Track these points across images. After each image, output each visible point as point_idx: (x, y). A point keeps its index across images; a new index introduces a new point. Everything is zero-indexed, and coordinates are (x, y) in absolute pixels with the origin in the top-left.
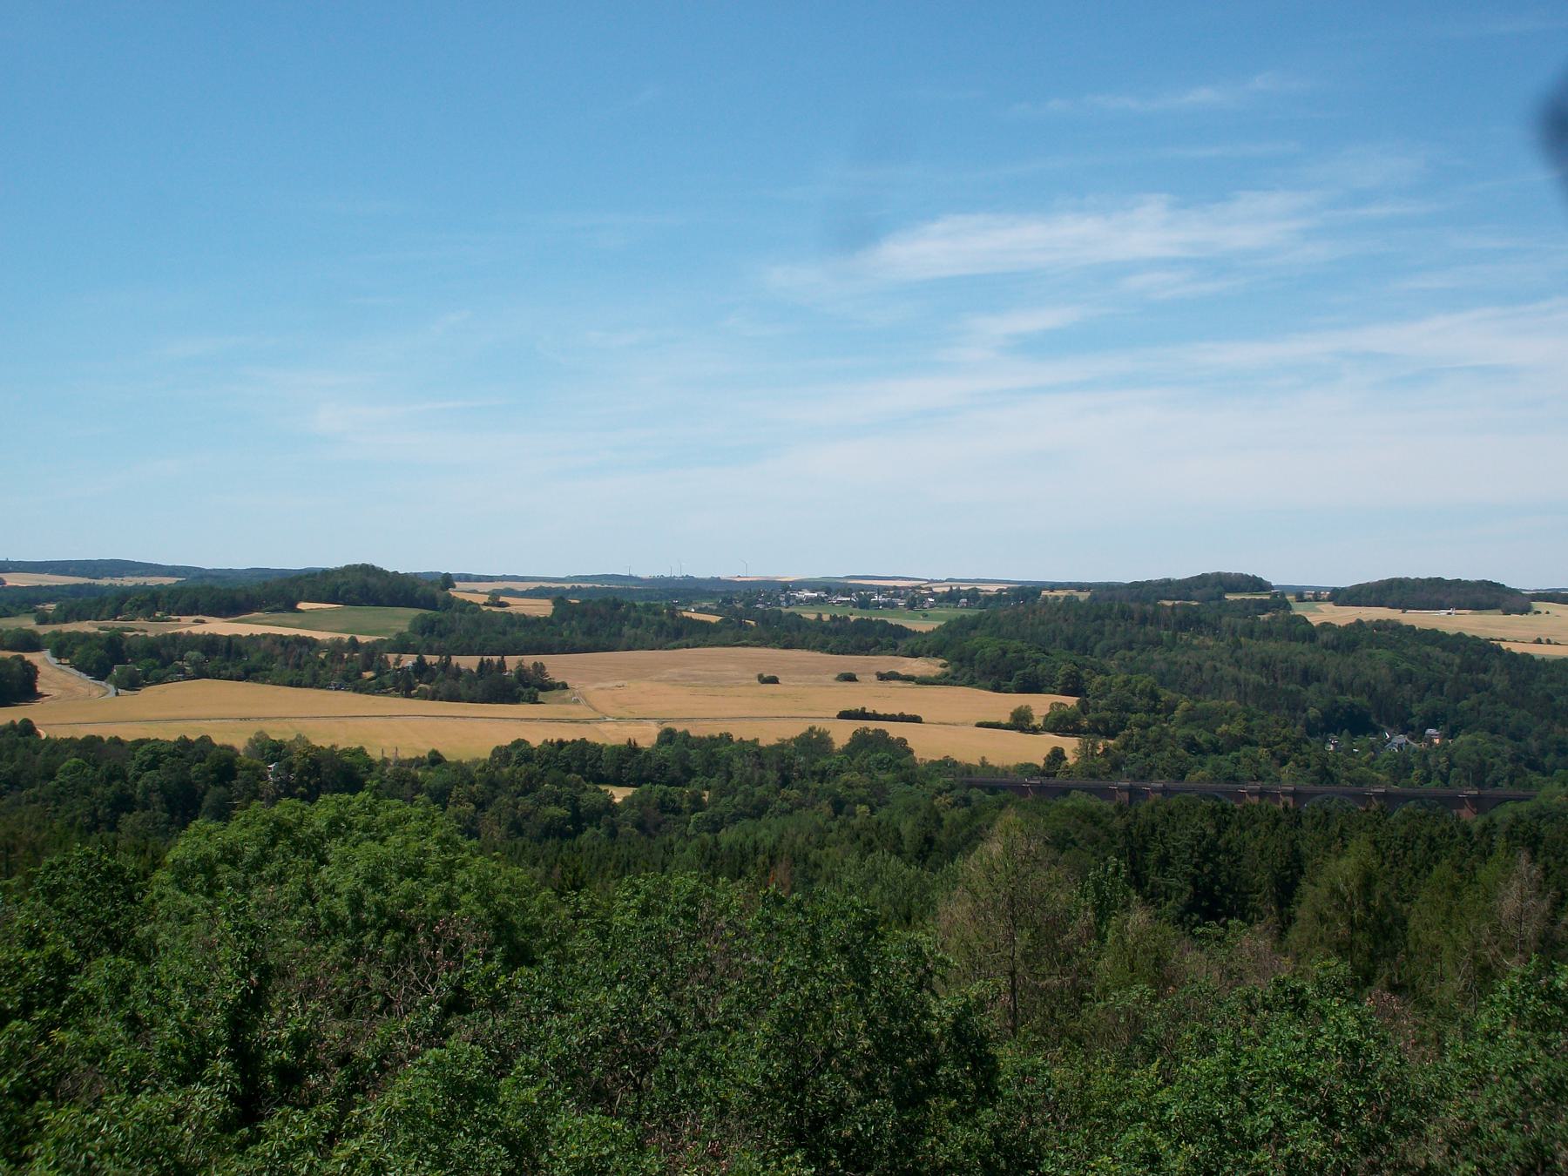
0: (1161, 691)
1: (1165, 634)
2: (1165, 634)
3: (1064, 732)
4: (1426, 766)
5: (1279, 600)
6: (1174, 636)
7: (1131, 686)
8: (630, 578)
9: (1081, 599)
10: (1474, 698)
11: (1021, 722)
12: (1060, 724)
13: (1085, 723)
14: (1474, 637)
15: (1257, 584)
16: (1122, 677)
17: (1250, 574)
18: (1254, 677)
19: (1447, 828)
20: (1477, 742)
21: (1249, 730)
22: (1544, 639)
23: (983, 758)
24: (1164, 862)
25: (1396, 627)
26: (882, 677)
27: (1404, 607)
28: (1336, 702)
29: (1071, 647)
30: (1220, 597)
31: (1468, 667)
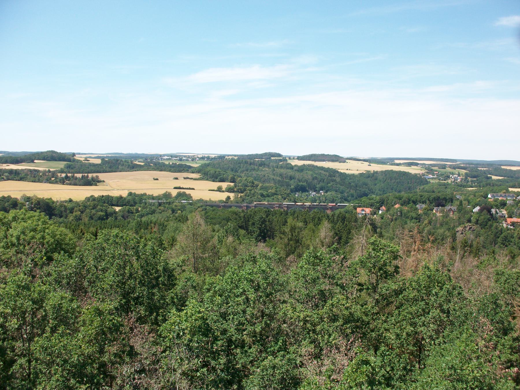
0: (255, 182)
1: (256, 167)
2: (256, 167)
3: (231, 192)
4: (320, 200)
5: (285, 160)
6: (258, 168)
7: (247, 180)
8: (121, 153)
10: (332, 183)
11: (220, 190)
12: (230, 190)
13: (236, 190)
14: (332, 169)
15: (279, 155)
16: (245, 178)
18: (278, 178)
19: (323, 215)
21: (276, 191)
24: (253, 224)
25: (313, 166)
26: (185, 178)
27: (315, 161)
29: (232, 171)
30: (270, 158)
31: (330, 176)
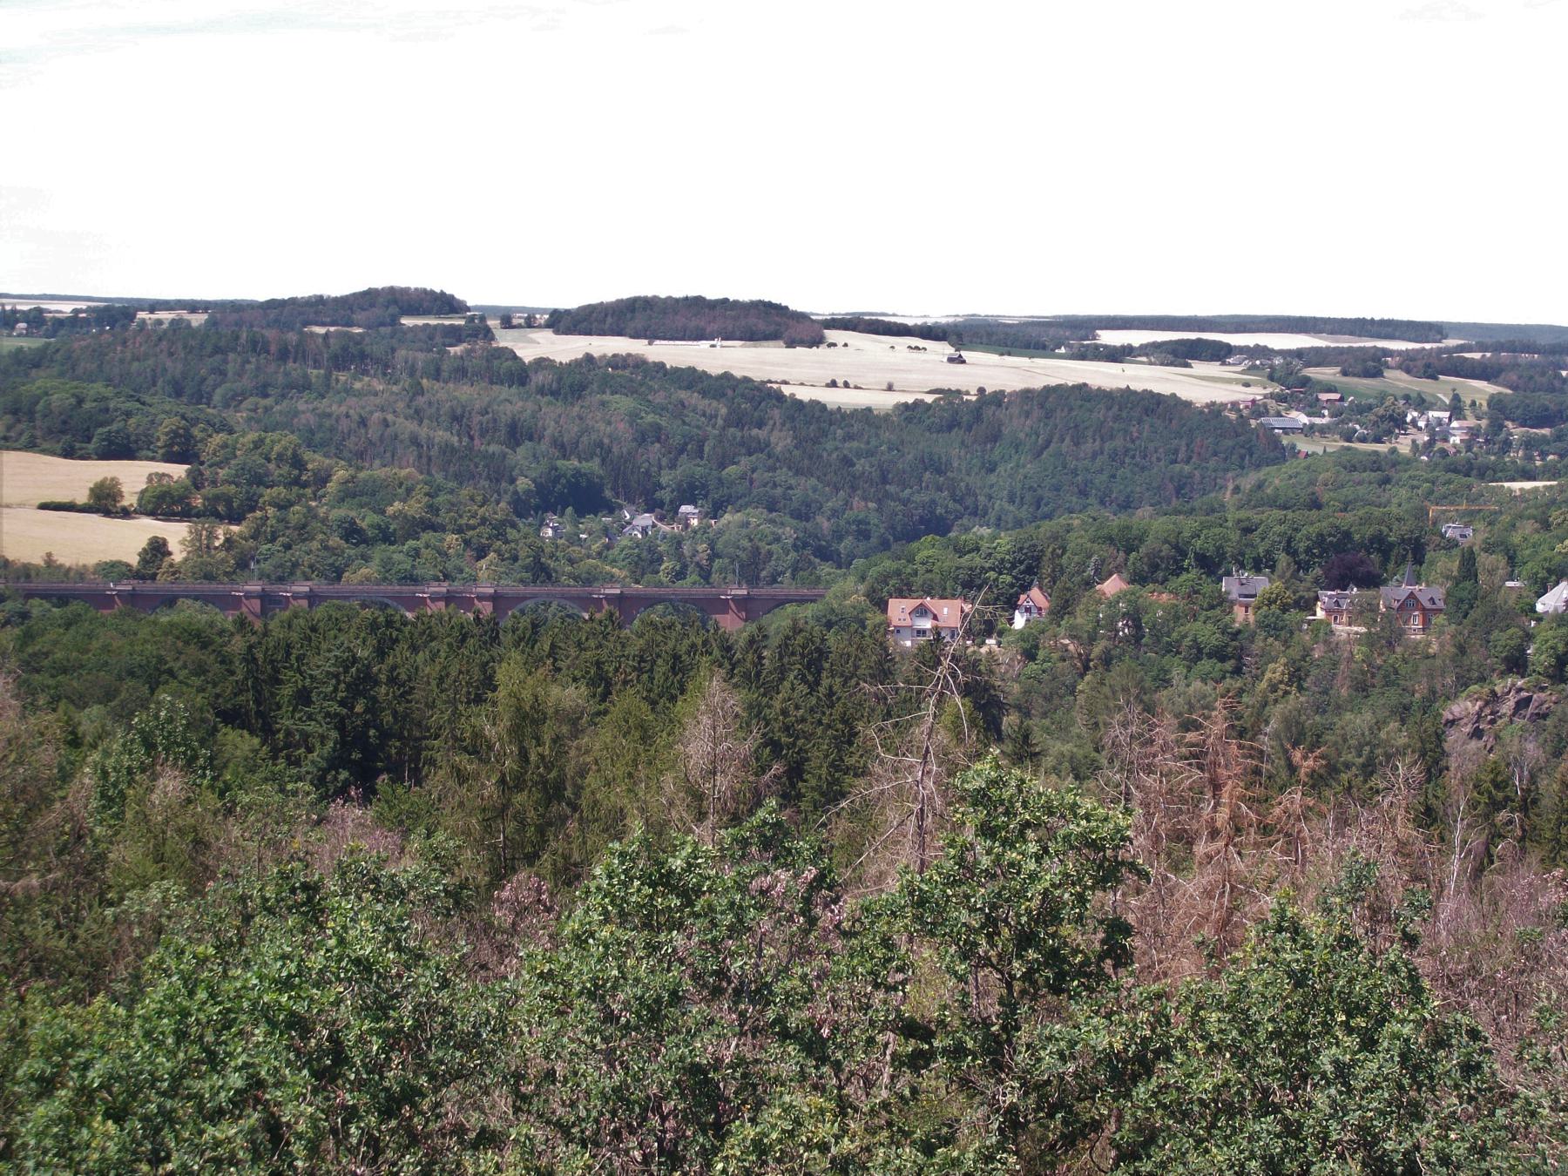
0: (307, 455)
1: (314, 373)
2: (314, 373)
3: (169, 516)
4: (680, 557)
5: (477, 326)
6: (328, 377)
7: (265, 449)
9: (195, 324)
10: (745, 462)
11: (104, 502)
12: (161, 504)
13: (198, 502)
14: (746, 380)
15: (446, 304)
16: (253, 436)
17: (438, 290)
18: (441, 435)
19: (699, 642)
20: (748, 523)
21: (433, 509)
22: (840, 382)
23: (49, 555)
24: (303, 697)
25: (639, 363)
27: (651, 335)
28: (556, 469)
29: (178, 392)
30: (394, 321)
31: (736, 419)
